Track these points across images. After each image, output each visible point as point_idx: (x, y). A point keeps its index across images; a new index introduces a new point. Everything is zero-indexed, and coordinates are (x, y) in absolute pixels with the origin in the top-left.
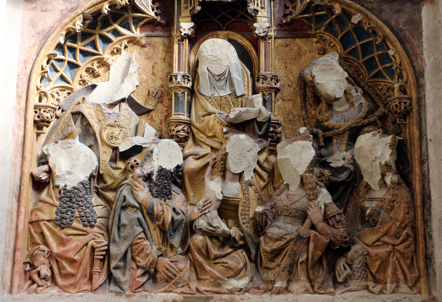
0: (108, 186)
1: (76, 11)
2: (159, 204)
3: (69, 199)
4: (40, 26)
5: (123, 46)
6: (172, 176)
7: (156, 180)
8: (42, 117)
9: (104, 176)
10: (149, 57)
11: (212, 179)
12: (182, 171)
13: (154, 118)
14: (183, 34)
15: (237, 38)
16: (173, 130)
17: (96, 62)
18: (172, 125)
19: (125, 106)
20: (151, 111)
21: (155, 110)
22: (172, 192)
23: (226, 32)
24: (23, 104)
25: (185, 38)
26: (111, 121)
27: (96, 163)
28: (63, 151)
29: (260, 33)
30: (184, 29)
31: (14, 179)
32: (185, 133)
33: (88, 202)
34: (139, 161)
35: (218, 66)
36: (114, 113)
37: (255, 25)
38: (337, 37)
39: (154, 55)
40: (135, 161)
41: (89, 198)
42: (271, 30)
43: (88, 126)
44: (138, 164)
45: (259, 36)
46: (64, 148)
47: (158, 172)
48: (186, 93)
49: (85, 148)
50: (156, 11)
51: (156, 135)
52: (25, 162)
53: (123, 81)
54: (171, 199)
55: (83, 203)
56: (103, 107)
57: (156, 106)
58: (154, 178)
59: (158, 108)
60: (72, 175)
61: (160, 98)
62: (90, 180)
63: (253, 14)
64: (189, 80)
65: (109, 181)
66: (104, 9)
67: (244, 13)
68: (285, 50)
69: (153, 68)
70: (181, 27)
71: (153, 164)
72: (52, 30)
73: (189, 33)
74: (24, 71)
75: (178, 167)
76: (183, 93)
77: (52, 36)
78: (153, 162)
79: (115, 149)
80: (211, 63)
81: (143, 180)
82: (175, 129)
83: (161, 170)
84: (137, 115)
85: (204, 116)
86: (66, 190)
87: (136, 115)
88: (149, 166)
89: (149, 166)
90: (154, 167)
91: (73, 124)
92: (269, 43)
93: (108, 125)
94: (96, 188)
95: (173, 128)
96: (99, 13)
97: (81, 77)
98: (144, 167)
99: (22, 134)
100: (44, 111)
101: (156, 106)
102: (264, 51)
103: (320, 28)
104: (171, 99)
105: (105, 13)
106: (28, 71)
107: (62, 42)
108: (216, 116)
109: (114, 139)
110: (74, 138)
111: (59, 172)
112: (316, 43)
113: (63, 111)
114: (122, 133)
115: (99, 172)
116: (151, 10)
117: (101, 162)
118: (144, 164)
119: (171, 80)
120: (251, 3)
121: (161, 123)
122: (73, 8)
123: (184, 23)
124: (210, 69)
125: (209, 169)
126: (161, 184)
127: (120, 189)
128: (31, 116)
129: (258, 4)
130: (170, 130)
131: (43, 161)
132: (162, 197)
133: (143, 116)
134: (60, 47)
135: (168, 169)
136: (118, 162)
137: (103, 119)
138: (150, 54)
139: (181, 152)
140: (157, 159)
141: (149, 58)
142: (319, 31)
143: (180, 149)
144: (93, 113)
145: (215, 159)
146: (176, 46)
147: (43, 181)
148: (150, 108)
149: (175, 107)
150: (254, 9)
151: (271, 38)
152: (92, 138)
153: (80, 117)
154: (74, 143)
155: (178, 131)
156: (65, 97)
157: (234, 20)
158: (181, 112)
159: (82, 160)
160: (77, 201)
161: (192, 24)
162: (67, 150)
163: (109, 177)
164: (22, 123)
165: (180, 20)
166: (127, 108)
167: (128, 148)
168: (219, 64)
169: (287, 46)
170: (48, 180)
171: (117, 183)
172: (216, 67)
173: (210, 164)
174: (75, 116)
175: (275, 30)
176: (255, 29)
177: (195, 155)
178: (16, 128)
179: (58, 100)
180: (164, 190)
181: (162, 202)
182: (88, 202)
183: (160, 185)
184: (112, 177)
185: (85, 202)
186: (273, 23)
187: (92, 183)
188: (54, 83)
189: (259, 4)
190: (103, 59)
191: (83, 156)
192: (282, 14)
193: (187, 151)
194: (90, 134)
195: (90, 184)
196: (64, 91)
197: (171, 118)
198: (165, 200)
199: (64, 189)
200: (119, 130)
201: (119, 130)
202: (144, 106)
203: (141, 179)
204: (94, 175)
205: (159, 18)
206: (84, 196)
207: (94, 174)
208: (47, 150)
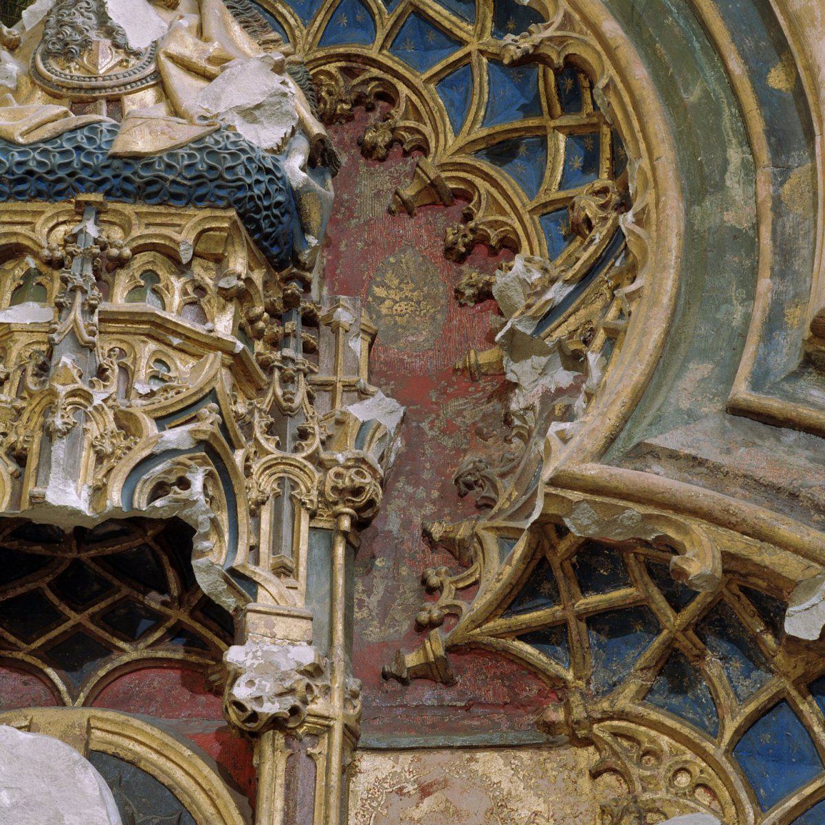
15: (139, 748)
29: (258, 699)
37: (234, 655)
38: (715, 734)
42: (327, 690)
45: (254, 716)
63: (229, 602)
67: (192, 615)
68: (417, 814)
92: (310, 756)
102: (279, 804)
103: (611, 688)
112: (595, 775)
120: (214, 538)
129: (254, 549)
142: (605, 705)
150: (232, 571)
151: (329, 729)
157: (134, 655)
169: (425, 791)
175: (355, 696)
176: (237, 676)
186: (339, 652)
189: (264, 548)
192: (406, 626)
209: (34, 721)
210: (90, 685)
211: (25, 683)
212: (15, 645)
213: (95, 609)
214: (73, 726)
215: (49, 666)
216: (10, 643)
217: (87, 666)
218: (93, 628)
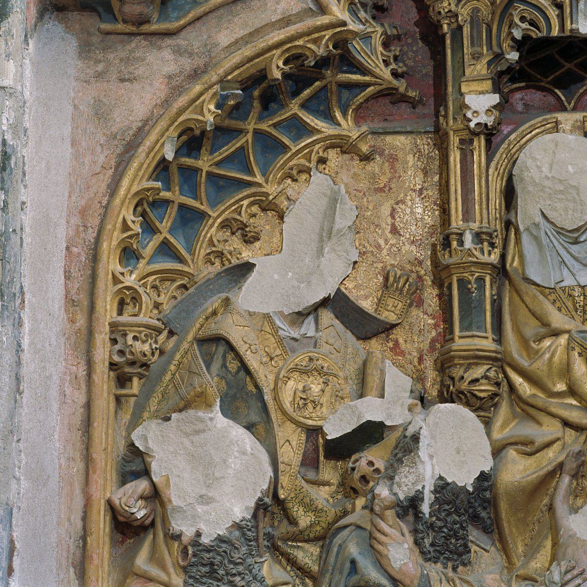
0: (301, 532)
1: (205, 78)
2: (443, 578)
3: (207, 569)
4: (118, 120)
5: (314, 158)
6: (469, 502)
7: (431, 516)
8: (132, 353)
9: (290, 505)
10: (382, 185)
11: (575, 510)
12: (491, 488)
13: (403, 346)
14: (472, 125)
16: (462, 378)
17: (245, 203)
18: (456, 364)
19: (327, 317)
20: (393, 326)
21: (404, 324)
22: (470, 544)
23: (579, 116)
24: (81, 321)
25: (477, 135)
26: (300, 359)
27: (270, 473)
28: (186, 442)
30: (475, 112)
31: (69, 519)
32: (492, 385)
33: (255, 578)
34: (380, 464)
35: (571, 205)
36: (304, 336)
39: (395, 180)
40: (371, 463)
41: (256, 566)
43: (242, 373)
44: (377, 471)
46: (187, 435)
47: (435, 492)
48: (488, 279)
49: (239, 433)
50: (393, 66)
51: (412, 392)
52: (94, 472)
53: (320, 252)
54: (470, 563)
55: (243, 578)
56: (278, 323)
57: (406, 312)
58: (425, 508)
59: (410, 320)
60: (212, 505)
61: (415, 292)
62: (255, 516)
64: (492, 245)
65: (304, 520)
66: (274, 66)
69: (392, 216)
70: (468, 108)
71: (421, 471)
72: (147, 128)
73: (490, 120)
74: (83, 235)
75: (483, 477)
76: (481, 280)
77: (148, 143)
78: (420, 466)
79: (314, 432)
80: (550, 198)
81: (398, 516)
82: (465, 377)
83: (442, 487)
84: (359, 338)
85: (540, 340)
86: (200, 545)
87: (354, 339)
88: (412, 478)
89: (412, 478)
90: (424, 479)
91: (204, 368)
93: (295, 369)
94: (269, 537)
95: (461, 372)
96: (262, 76)
97: (211, 243)
98: (397, 477)
99: (82, 399)
100: (135, 338)
101: (406, 312)
104: (450, 296)
105: (278, 79)
106: (91, 235)
107: (170, 156)
108: (571, 339)
109: (310, 406)
110: (209, 406)
111: (179, 497)
113: (171, 333)
114: (327, 389)
115: (275, 496)
116: (382, 65)
117: (281, 467)
118: (395, 471)
119: (446, 243)
121: (421, 360)
122: (199, 68)
123: (473, 96)
124: (550, 214)
125: (566, 479)
126: (445, 526)
127: (338, 540)
128: (103, 352)
130: (453, 379)
131: (135, 467)
132: (448, 559)
133: (373, 341)
134: (162, 168)
135: (460, 484)
136: (321, 466)
137: (278, 352)
138: (384, 180)
139: (486, 437)
140: (431, 457)
141: (381, 190)
143: (482, 426)
144: (252, 336)
145: (580, 453)
146: (455, 157)
147: (138, 523)
148: (392, 318)
149: (462, 318)
152: (255, 405)
153: (221, 349)
154: (211, 419)
155: (475, 381)
156: (175, 297)
158: (479, 328)
159: (235, 463)
160: (227, 574)
161: (495, 99)
162: (196, 438)
163: (301, 509)
164: (82, 372)
165: (464, 89)
166: (334, 323)
167: (349, 430)
168: (574, 201)
170: (150, 519)
171: (324, 526)
172: (566, 209)
173: (568, 467)
174: (205, 347)
177: (524, 444)
178: (67, 384)
179: (157, 306)
180: (453, 541)
181: (451, 574)
182: (255, 578)
183: (441, 528)
184: (310, 507)
185: (248, 578)
187: (261, 525)
188: (148, 263)
190: (266, 194)
191: (236, 453)
193: (497, 435)
194: (247, 394)
195: (257, 527)
196: (173, 280)
197: (455, 346)
198: (455, 569)
199: (196, 541)
200: (322, 380)
201: (322, 380)
202: (374, 315)
203: (390, 514)
204: (265, 504)
205: (401, 85)
206: (244, 560)
207: (267, 500)
208: (145, 439)
209: (559, 119)
210: (576, 97)
211: (545, 96)
212: (540, 79)
213: (578, 61)
214: (577, 121)
215: (557, 88)
216: (538, 78)
217: (572, 87)
218: (576, 70)
